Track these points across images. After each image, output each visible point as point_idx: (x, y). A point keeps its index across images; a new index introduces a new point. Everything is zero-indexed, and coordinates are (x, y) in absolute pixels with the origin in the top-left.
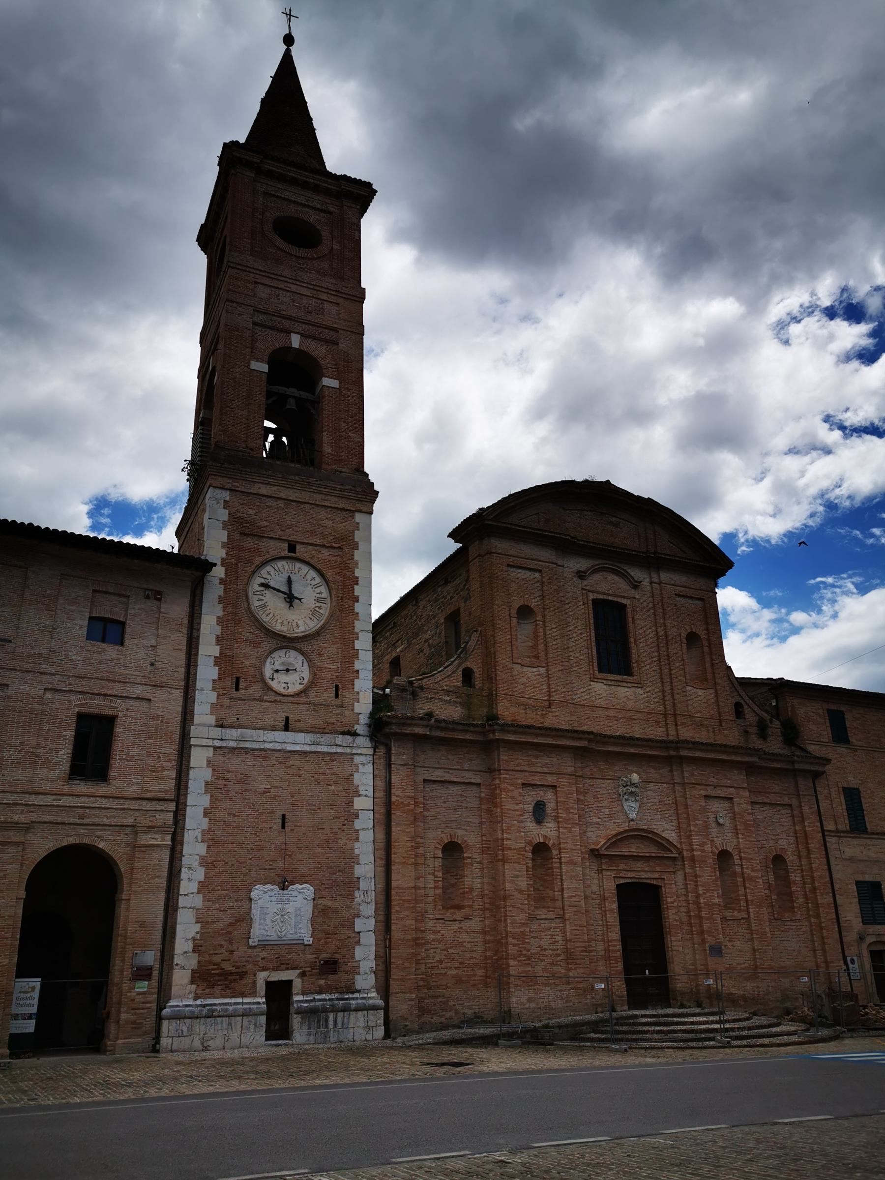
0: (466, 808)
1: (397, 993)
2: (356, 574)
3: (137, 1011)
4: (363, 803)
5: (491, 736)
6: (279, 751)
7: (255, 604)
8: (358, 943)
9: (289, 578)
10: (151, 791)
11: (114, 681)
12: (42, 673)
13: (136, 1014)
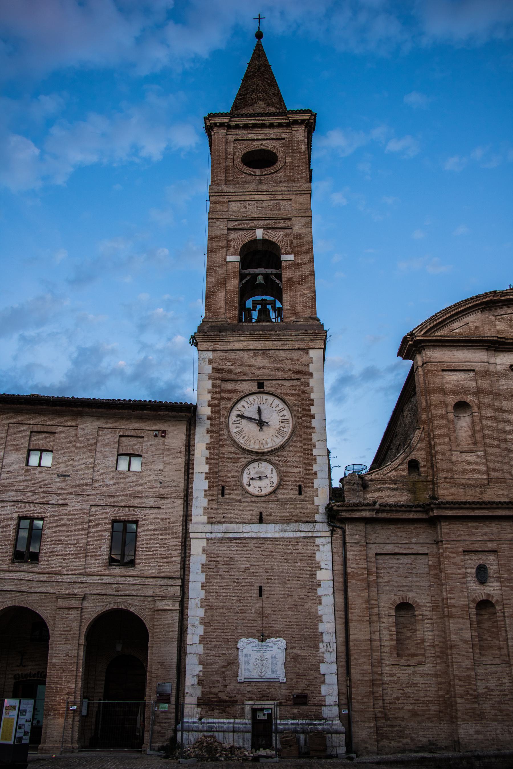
0: (416, 574)
1: (358, 722)
2: (312, 397)
3: (162, 725)
4: (324, 575)
5: (431, 514)
6: (255, 538)
7: (233, 430)
8: (323, 682)
9: (259, 408)
10: (163, 572)
11: (135, 497)
12: (88, 495)
13: (160, 726)
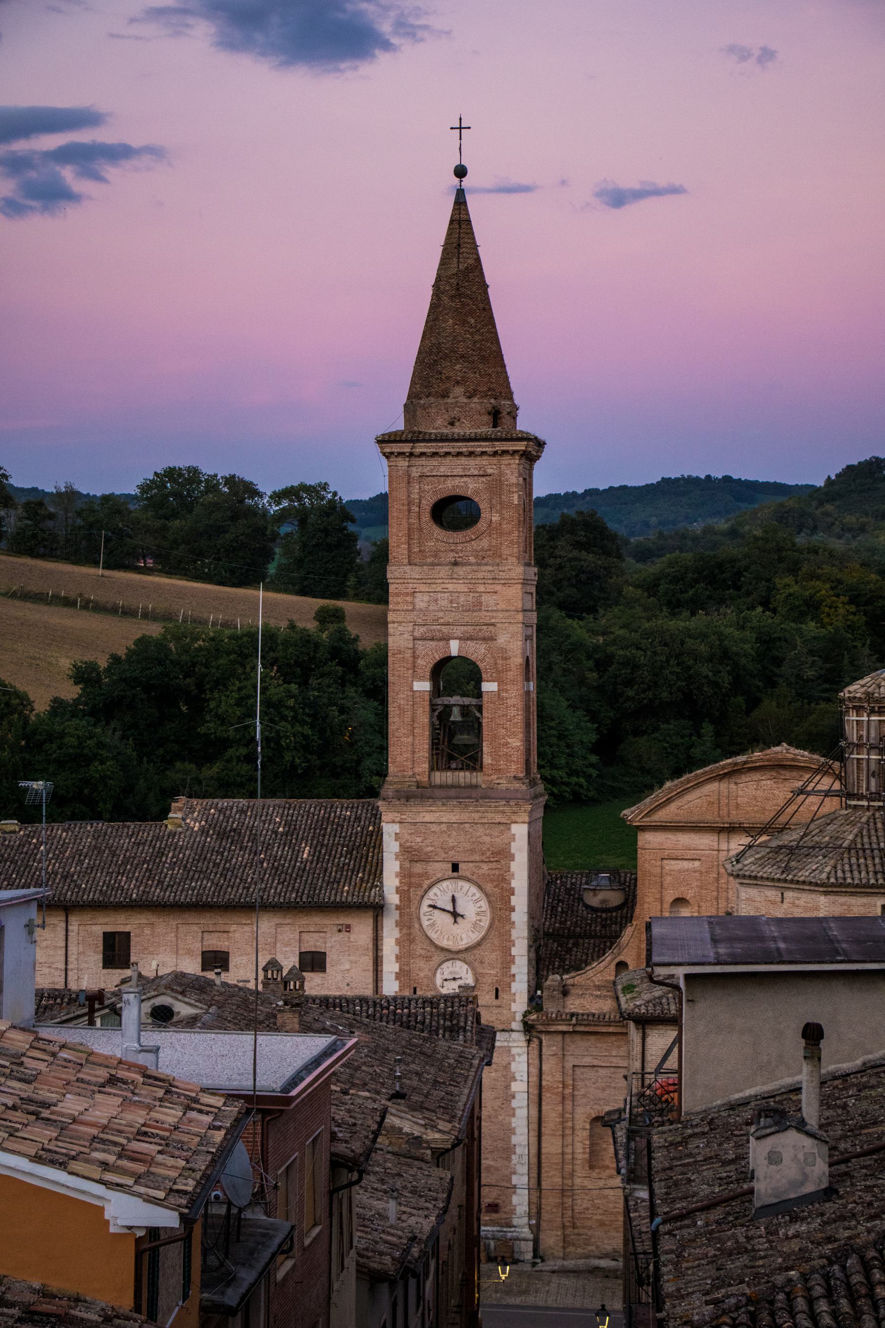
0: (615, 1088)
2: (513, 885)
4: (519, 1087)
7: (425, 923)
9: (453, 897)
